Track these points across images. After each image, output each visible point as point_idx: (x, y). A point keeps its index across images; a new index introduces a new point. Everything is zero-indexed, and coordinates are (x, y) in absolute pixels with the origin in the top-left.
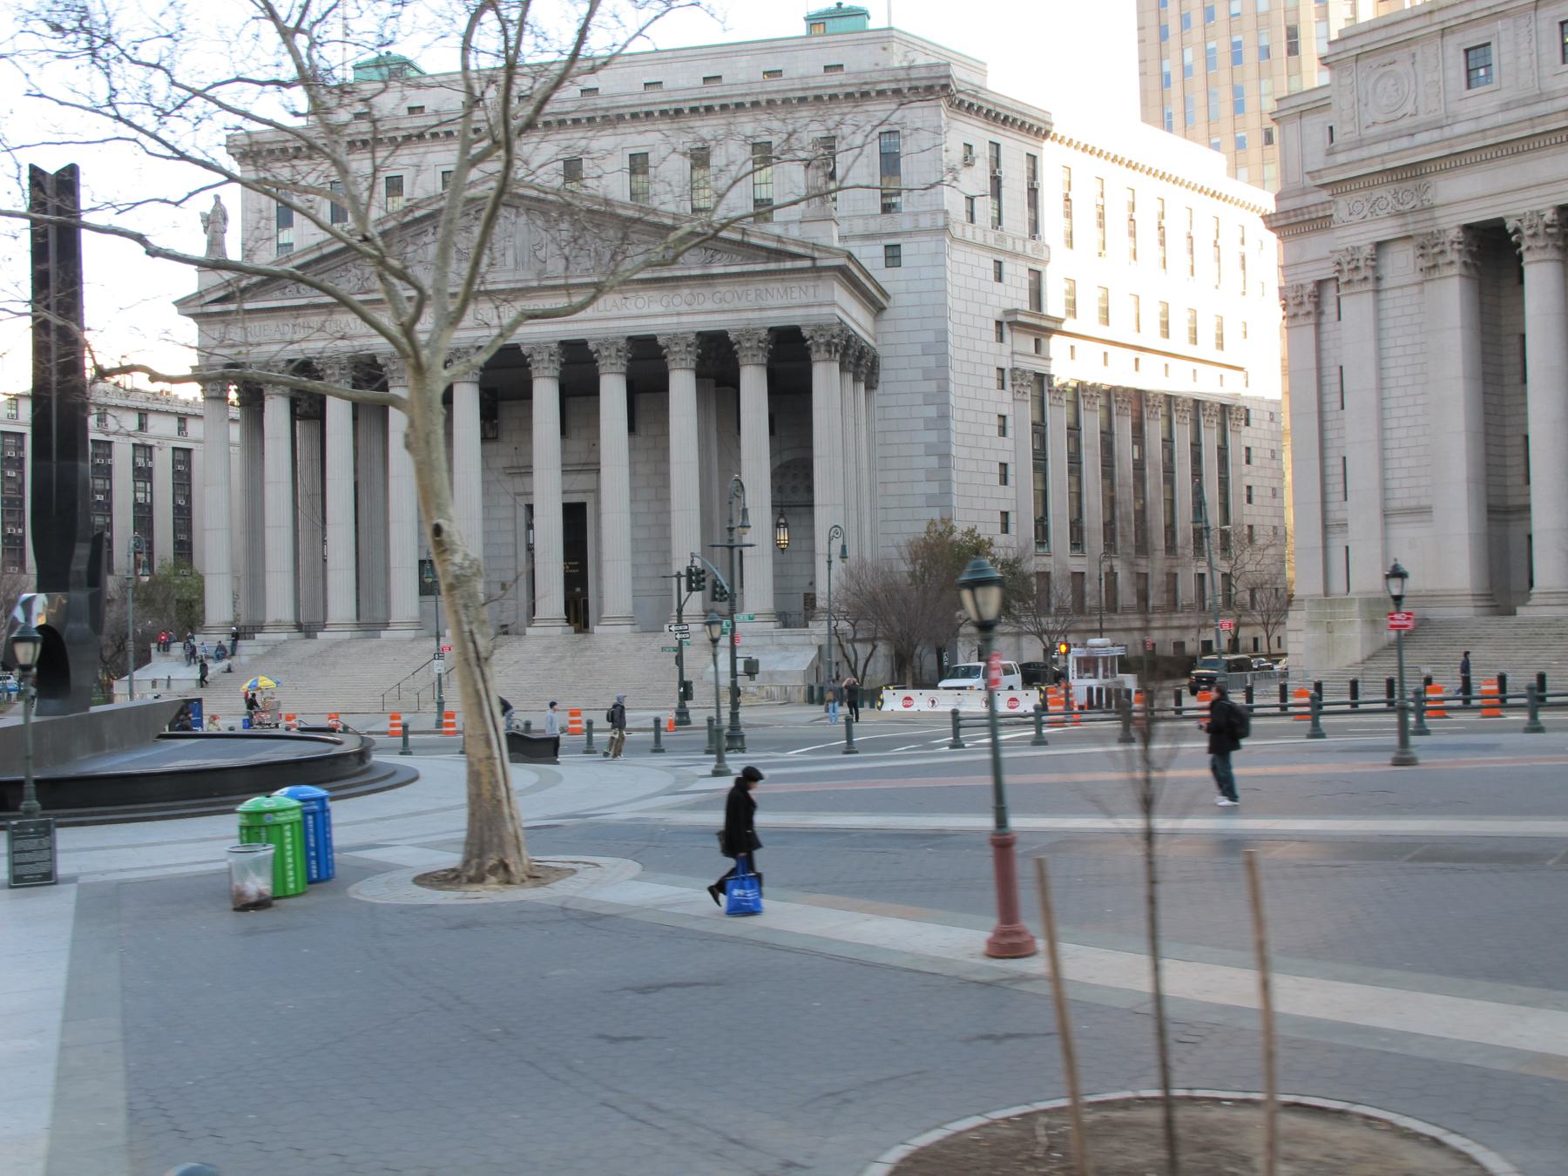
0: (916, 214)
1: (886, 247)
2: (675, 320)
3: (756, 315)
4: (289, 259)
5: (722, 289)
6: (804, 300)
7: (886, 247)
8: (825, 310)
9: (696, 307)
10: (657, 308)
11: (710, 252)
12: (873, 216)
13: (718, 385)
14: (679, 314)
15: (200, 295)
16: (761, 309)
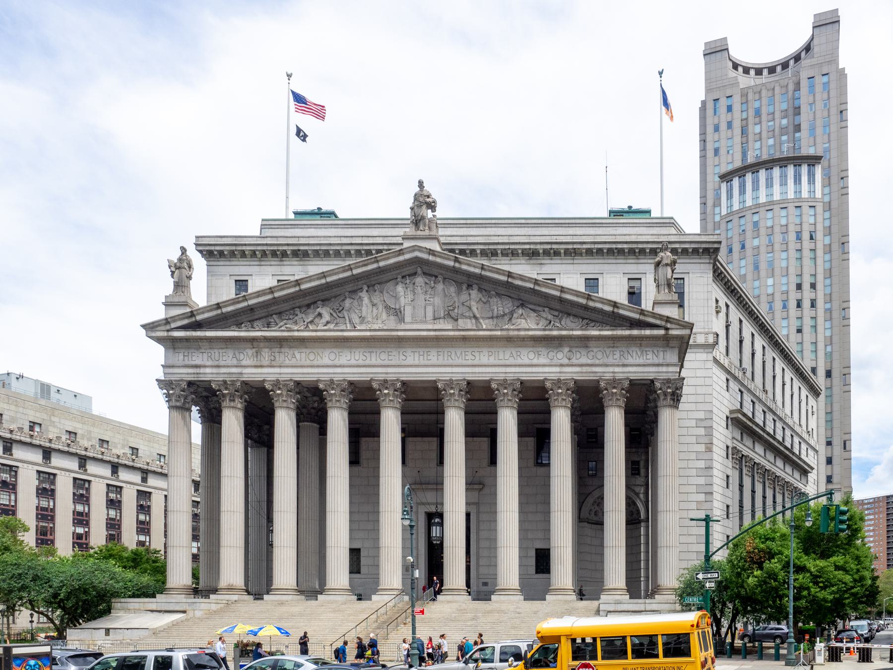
2: (557, 369)
4: (245, 299)
5: (595, 350)
6: (656, 361)
9: (574, 361)
10: (542, 360)
11: (585, 321)
14: (562, 365)
15: (167, 321)
16: (624, 365)
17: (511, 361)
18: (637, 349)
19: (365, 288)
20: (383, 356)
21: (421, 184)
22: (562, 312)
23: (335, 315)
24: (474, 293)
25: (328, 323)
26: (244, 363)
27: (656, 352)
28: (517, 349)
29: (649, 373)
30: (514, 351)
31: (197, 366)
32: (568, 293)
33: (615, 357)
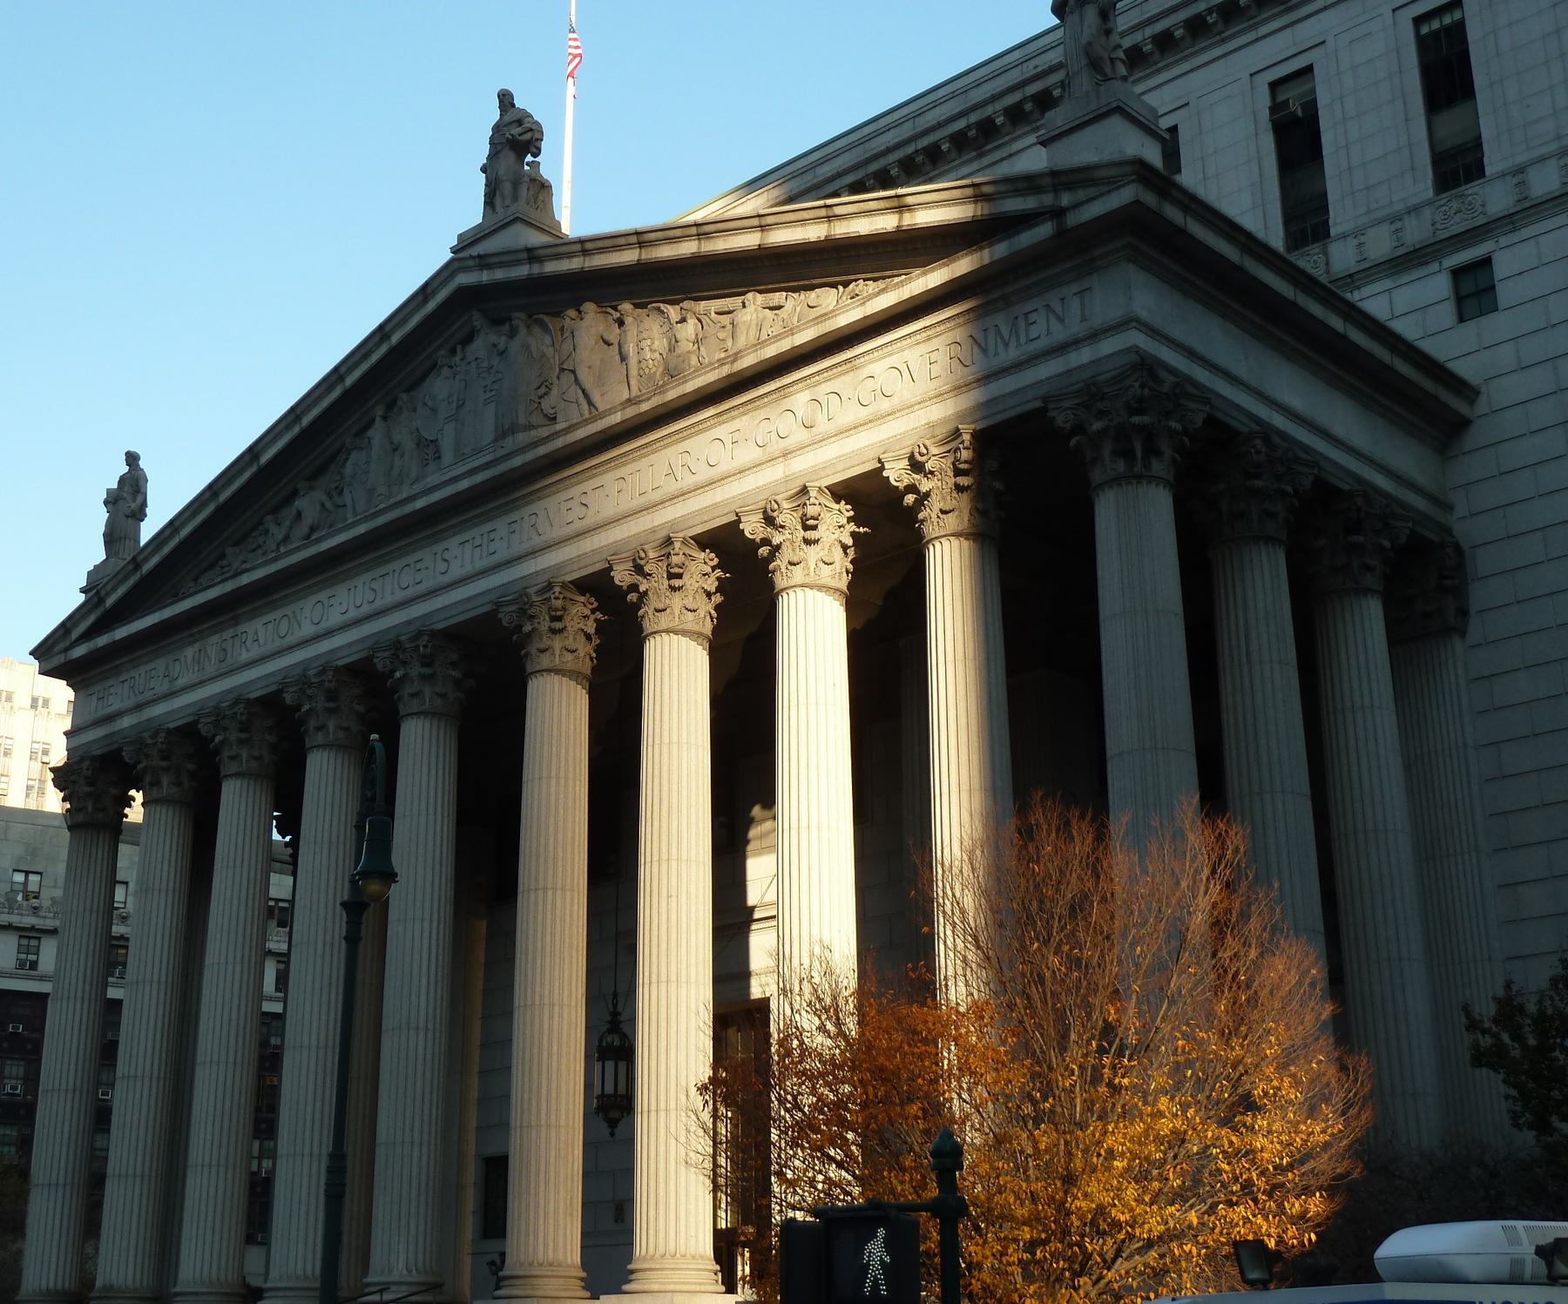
0: (1520, 170)
1: (1457, 273)
6: (1060, 334)
7: (1457, 273)
8: (1108, 346)
12: (1414, 210)
20: (407, 578)
21: (506, 100)
23: (328, 505)
25: (313, 529)
26: (181, 682)
31: (110, 718)
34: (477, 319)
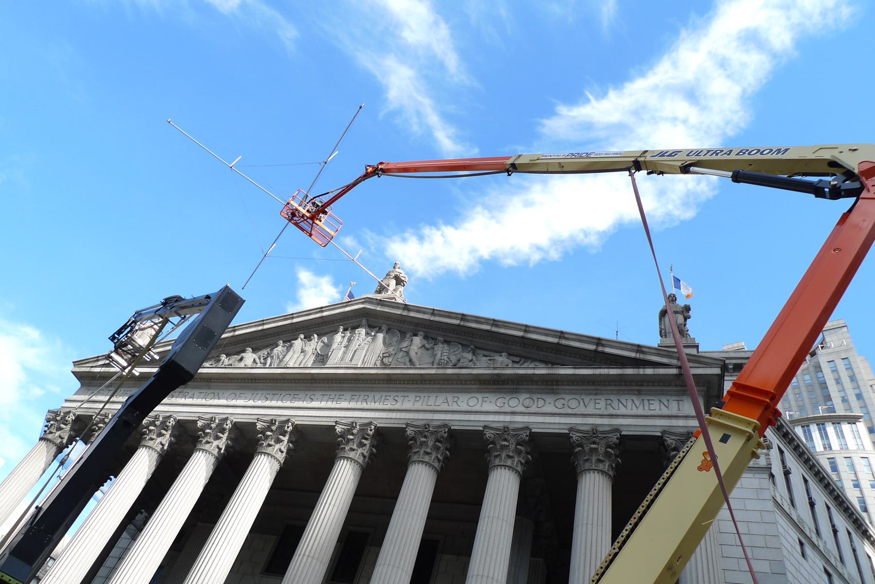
2: (508, 418)
3: (606, 421)
5: (567, 397)
6: (665, 411)
13: (532, 555)
14: (513, 413)
16: (611, 416)
17: (444, 407)
18: (635, 398)
19: (302, 336)
22: (524, 357)
24: (417, 341)
27: (666, 403)
28: (455, 395)
29: (653, 426)
30: (450, 397)
32: (533, 332)
33: (598, 406)
34: (364, 322)
